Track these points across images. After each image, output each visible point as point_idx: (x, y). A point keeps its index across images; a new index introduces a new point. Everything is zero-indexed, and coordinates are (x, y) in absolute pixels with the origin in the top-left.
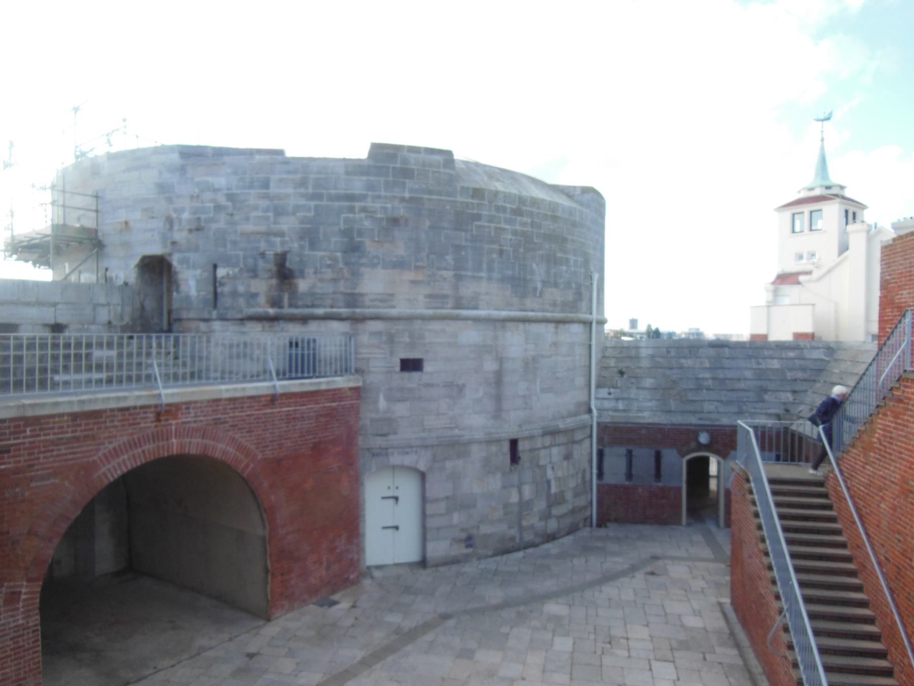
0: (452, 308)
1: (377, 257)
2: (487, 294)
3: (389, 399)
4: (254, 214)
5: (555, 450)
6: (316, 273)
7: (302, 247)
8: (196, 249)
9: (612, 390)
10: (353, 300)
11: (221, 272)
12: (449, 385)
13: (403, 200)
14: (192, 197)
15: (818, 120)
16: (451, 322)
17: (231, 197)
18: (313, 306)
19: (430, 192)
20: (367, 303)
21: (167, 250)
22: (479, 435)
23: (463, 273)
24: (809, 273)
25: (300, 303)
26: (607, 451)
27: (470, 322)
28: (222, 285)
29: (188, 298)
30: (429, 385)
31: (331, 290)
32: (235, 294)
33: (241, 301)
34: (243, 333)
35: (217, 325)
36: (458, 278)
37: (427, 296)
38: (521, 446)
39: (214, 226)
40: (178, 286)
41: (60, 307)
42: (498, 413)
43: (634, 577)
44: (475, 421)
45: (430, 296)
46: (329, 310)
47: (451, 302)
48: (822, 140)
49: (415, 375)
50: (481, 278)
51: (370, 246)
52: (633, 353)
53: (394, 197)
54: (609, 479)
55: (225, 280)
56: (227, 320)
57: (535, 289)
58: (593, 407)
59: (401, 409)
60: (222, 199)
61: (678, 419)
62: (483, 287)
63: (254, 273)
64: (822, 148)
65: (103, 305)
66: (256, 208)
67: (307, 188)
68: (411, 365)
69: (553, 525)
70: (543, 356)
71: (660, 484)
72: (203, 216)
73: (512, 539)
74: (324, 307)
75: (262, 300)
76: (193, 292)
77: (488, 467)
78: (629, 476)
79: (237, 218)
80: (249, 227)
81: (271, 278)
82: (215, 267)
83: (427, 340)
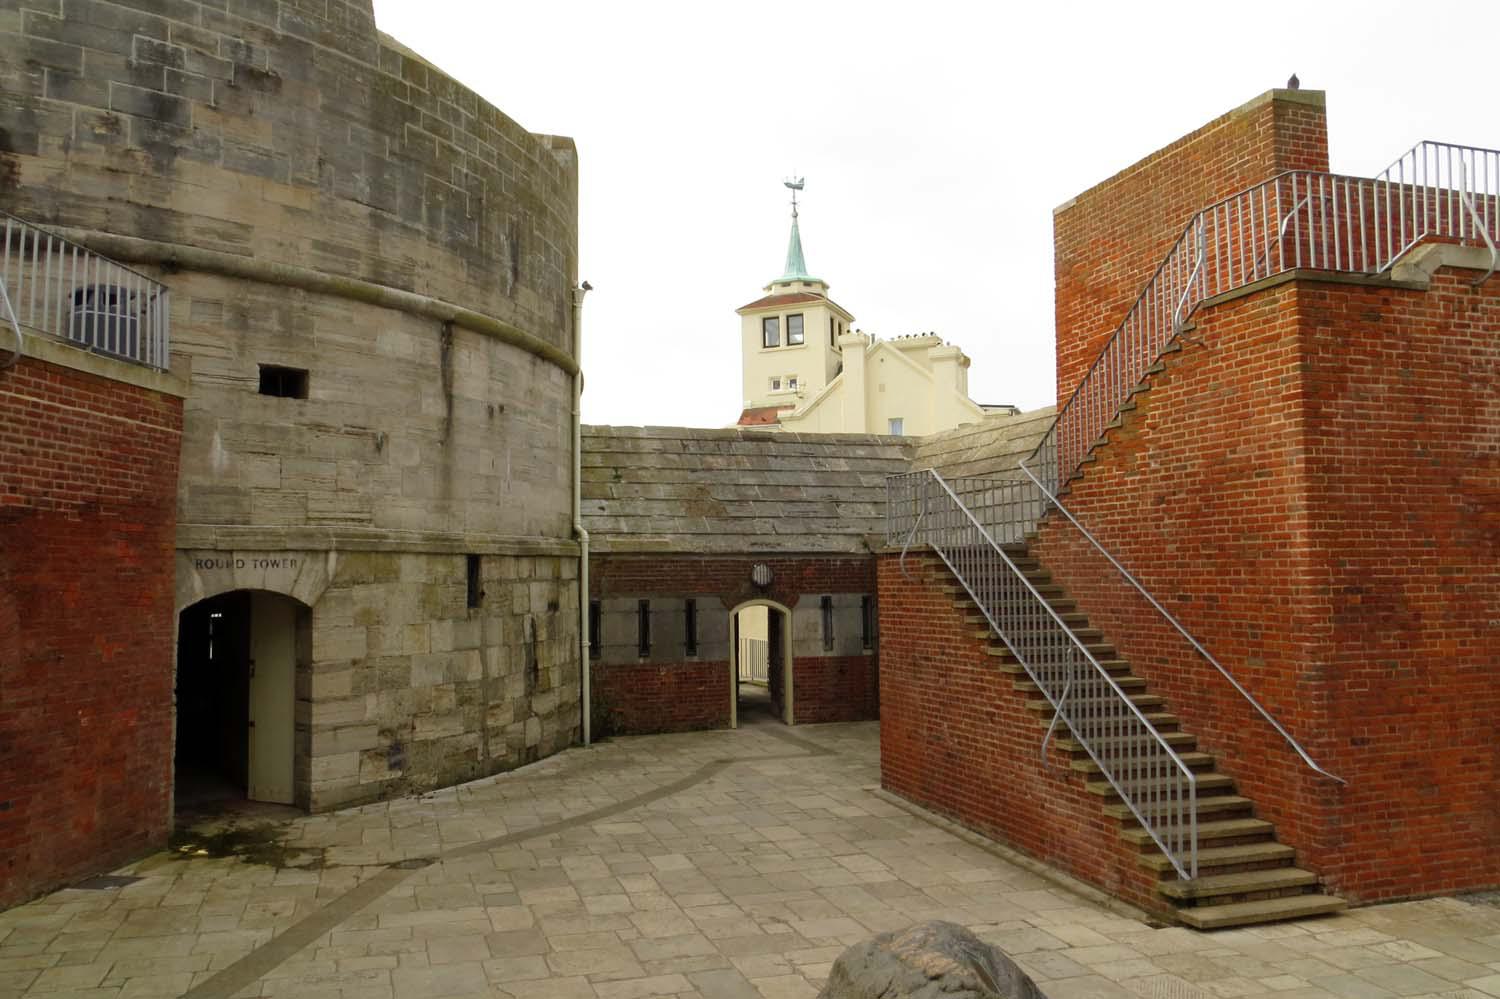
0: (364, 279)
1: (214, 141)
3: (232, 446)
5: (535, 588)
6: (66, 148)
7: (31, 84)
9: (604, 503)
10: (155, 219)
12: (358, 432)
13: (269, 38)
15: (788, 185)
16: (365, 308)
19: (326, 41)
22: (414, 538)
26: (606, 604)
27: (398, 315)
30: (319, 427)
31: (102, 193)
36: (378, 222)
37: (317, 244)
38: (487, 571)
42: (445, 502)
43: (711, 782)
44: (407, 513)
46: (100, 235)
48: (795, 216)
49: (291, 402)
50: (418, 232)
51: (195, 113)
52: (629, 446)
54: (609, 657)
58: (579, 527)
59: (259, 472)
61: (721, 545)
62: (421, 251)
64: (796, 226)
68: (283, 383)
69: (534, 731)
71: (696, 659)
73: (471, 753)
77: (429, 604)
78: (644, 647)
83: (317, 334)
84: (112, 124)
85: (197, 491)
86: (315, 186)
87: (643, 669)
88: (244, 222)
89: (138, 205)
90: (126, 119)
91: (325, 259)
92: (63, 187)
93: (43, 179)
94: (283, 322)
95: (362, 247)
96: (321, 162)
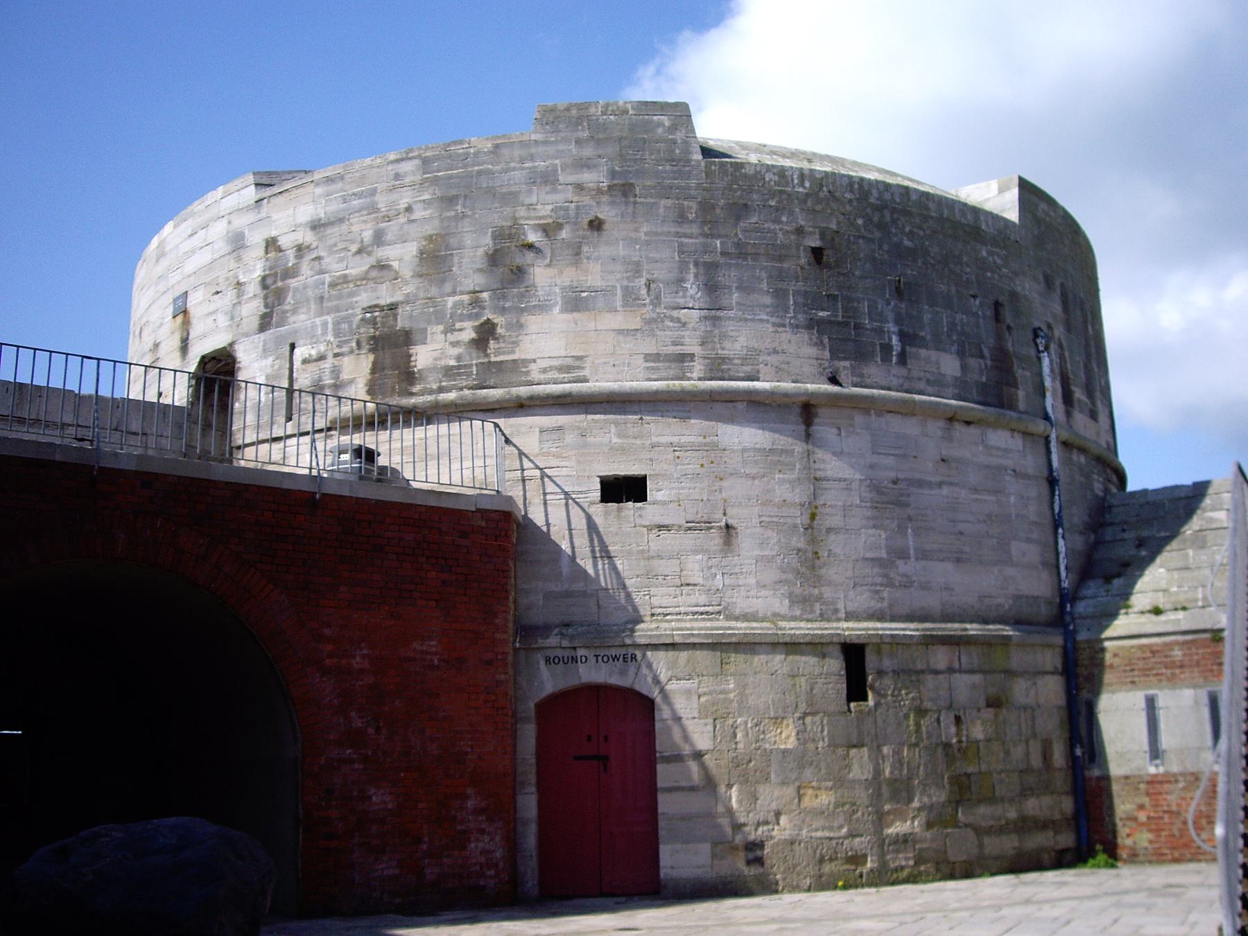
0: (700, 379)
2: (775, 352)
37: (648, 357)
38: (871, 662)
47: (698, 368)
57: (887, 348)
70: (920, 483)
78: (1155, 752)
85: (548, 596)
87: (1153, 781)
88: (580, 354)
91: (658, 369)
95: (696, 350)
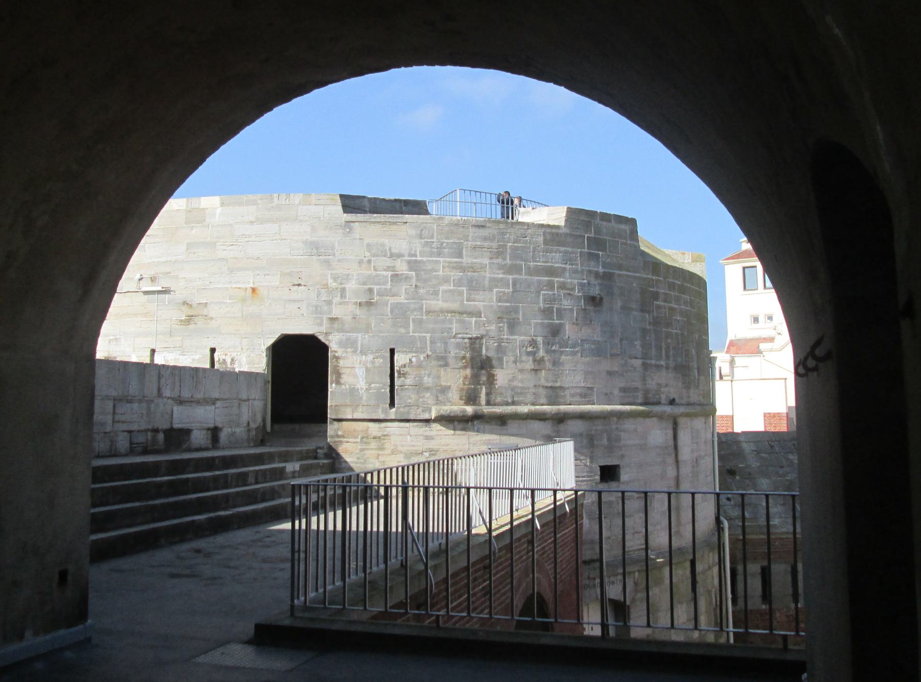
4: (443, 288)
6: (515, 362)
7: (500, 330)
8: (367, 329)
11: (400, 359)
14: (361, 262)
16: (640, 420)
17: (414, 265)
18: (513, 403)
19: (620, 267)
20: (569, 399)
21: (323, 329)
23: (649, 362)
24: (771, 340)
25: (499, 399)
28: (403, 375)
29: (353, 391)
32: (419, 387)
33: (428, 397)
34: (427, 438)
35: (394, 428)
39: (392, 300)
40: (338, 375)
41: (218, 404)
45: (624, 390)
46: (533, 408)
50: (662, 366)
53: (590, 271)
55: (406, 370)
56: (408, 421)
60: (402, 267)
63: (443, 360)
65: (244, 401)
66: (446, 280)
67: (505, 259)
72: (376, 288)
74: (526, 404)
75: (454, 395)
76: (361, 384)
79: (421, 291)
80: (438, 304)
81: (465, 367)
82: (392, 352)
83: (623, 442)
84: (533, 343)
86: (618, 355)
89: (547, 387)
90: (540, 340)
92: (515, 383)
93: (506, 381)
94: (609, 439)
95: (638, 384)
96: (621, 340)
